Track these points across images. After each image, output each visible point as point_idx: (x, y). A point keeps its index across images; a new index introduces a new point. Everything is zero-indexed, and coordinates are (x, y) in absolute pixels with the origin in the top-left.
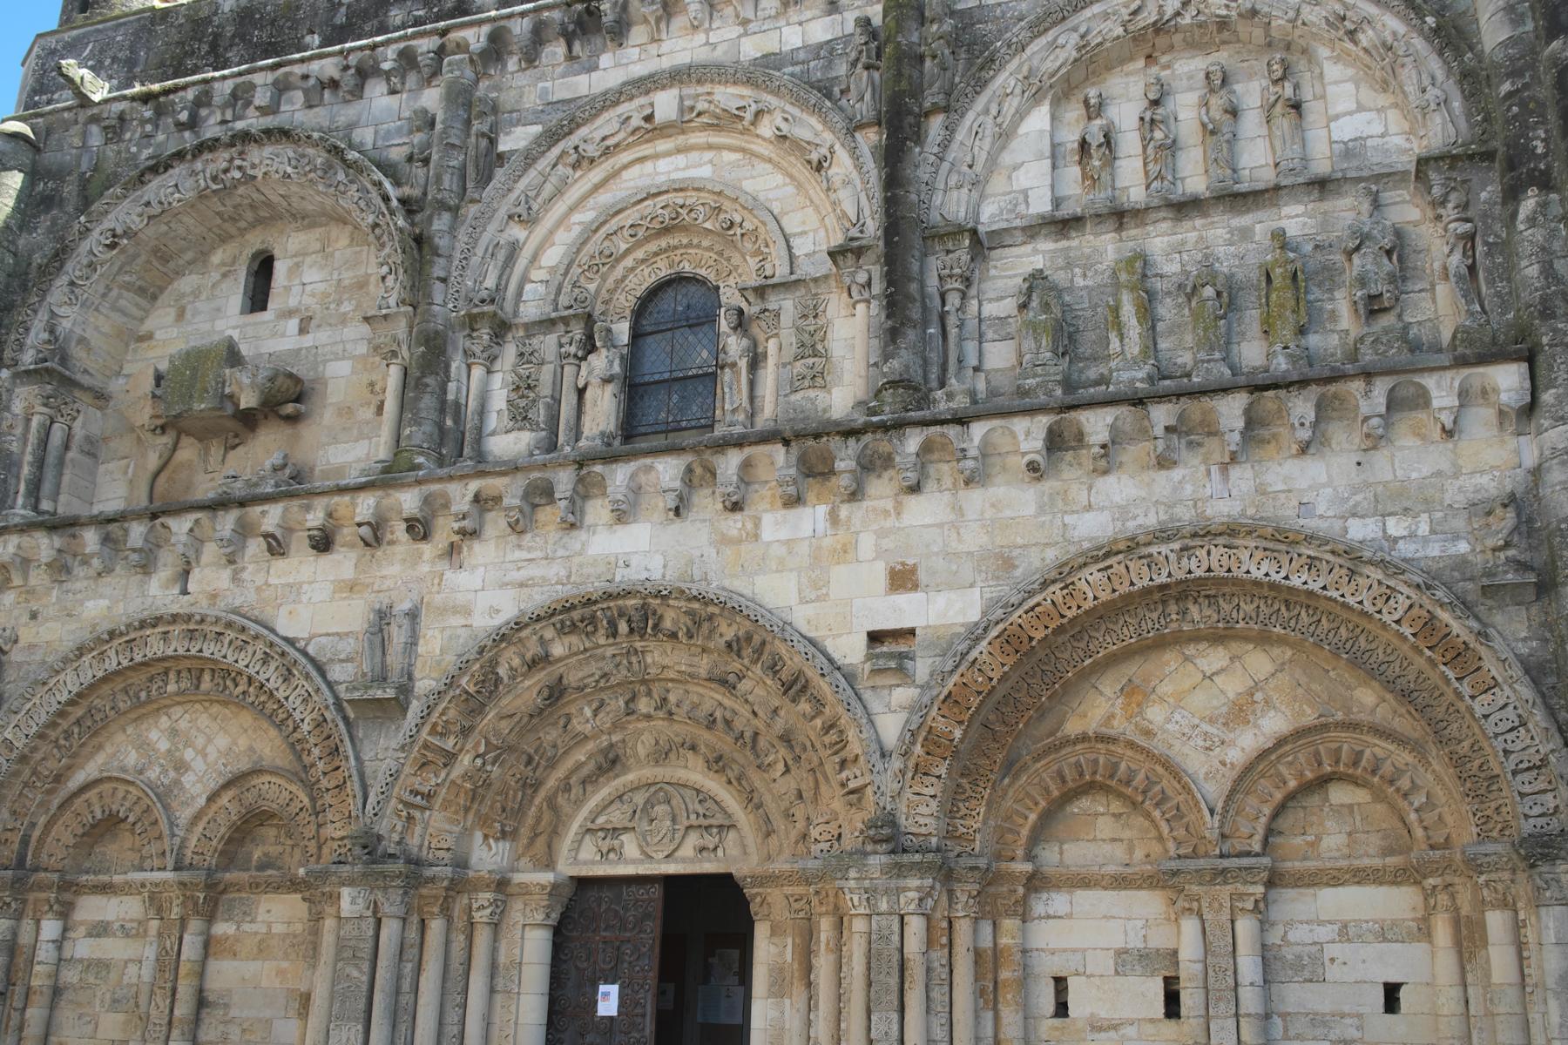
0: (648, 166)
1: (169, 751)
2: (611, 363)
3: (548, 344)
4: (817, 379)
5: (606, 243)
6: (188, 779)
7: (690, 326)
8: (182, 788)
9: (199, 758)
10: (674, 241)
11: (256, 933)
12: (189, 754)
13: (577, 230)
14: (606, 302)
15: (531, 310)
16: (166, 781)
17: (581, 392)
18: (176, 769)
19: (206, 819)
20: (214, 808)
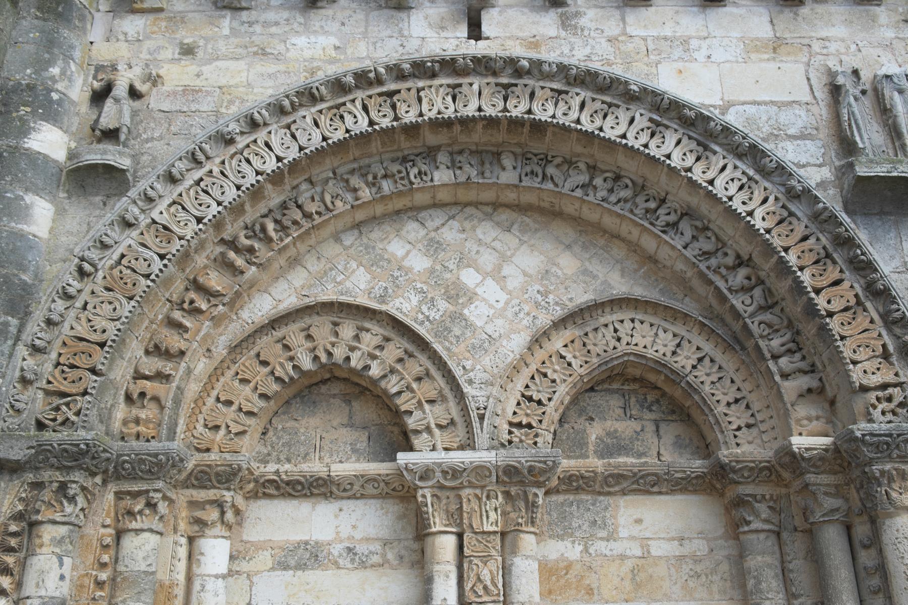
1: (432, 271)
6: (476, 313)
8: (468, 325)
9: (489, 282)
11: (623, 557)
12: (469, 278)
16: (432, 314)
18: (449, 298)
19: (526, 373)
20: (540, 355)
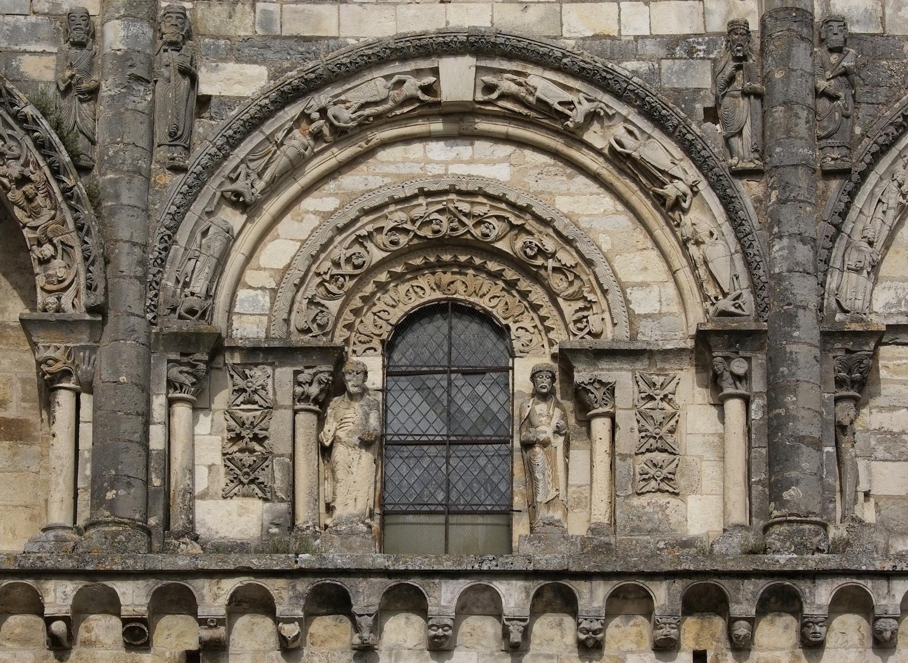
0: (416, 150)
2: (367, 415)
3: (279, 381)
4: (669, 485)
5: (357, 249)
7: (464, 373)
10: (447, 257)
13: (314, 221)
14: (349, 327)
15: (249, 327)
17: (326, 451)
